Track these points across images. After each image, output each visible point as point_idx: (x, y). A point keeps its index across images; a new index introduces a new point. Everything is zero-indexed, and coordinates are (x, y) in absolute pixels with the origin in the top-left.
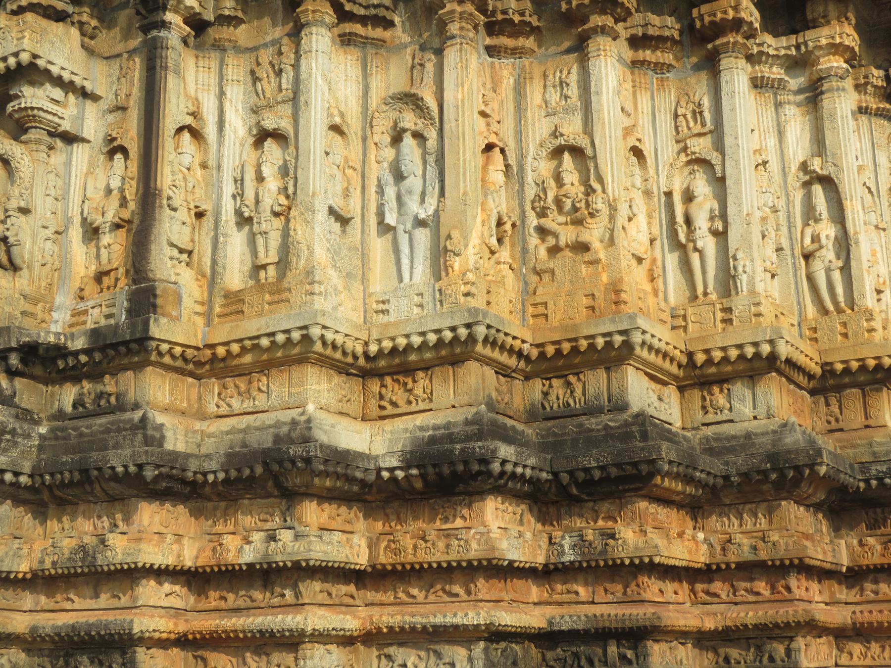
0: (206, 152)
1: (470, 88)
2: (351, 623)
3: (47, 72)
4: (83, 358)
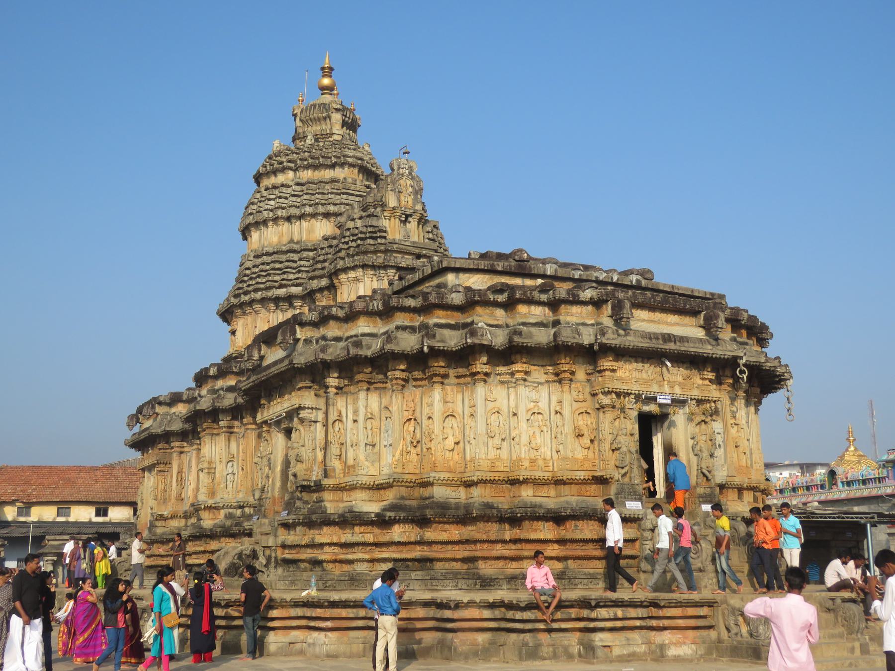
0: (344, 424)
2: (367, 556)
3: (305, 407)
4: (314, 488)
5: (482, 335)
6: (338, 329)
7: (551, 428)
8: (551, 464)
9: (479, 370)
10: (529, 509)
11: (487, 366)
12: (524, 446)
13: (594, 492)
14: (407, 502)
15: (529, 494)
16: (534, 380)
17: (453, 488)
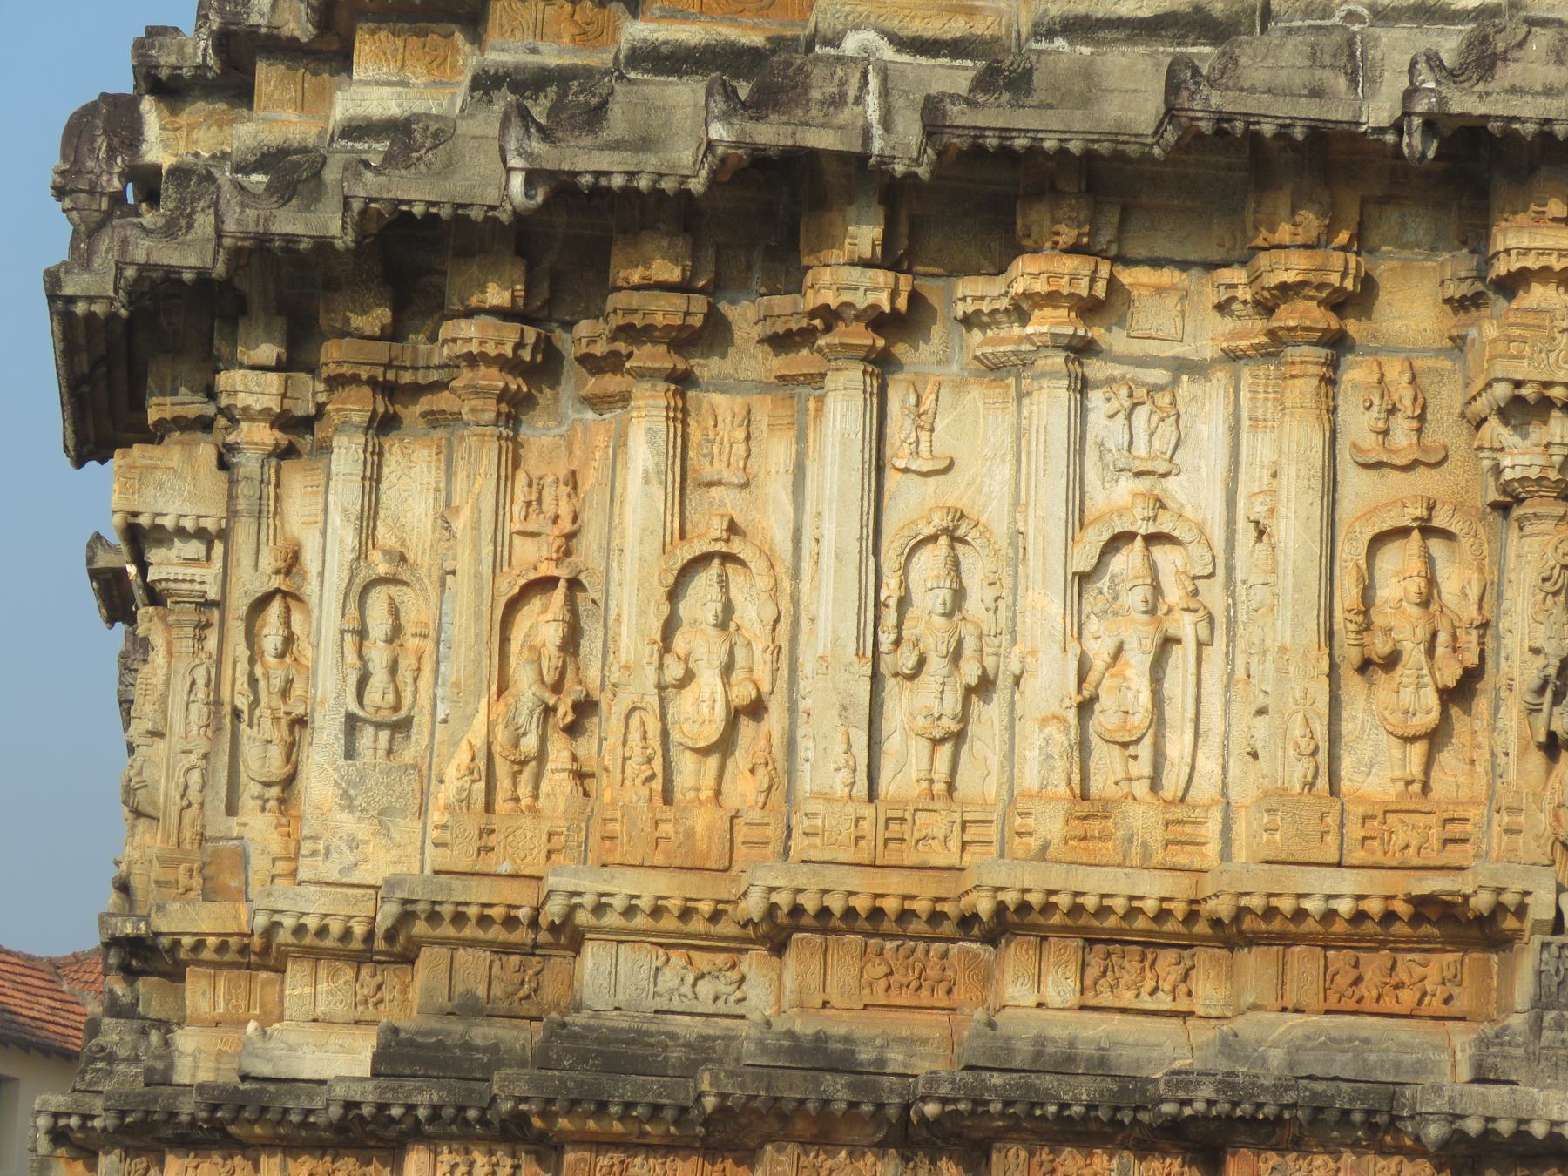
1: (477, 509)
5: (838, 101)
6: (301, 105)
7: (1231, 623)
8: (1212, 829)
9: (830, 298)
10: (997, 1080)
11: (882, 277)
12: (1044, 722)
13: (1441, 992)
14: (483, 1033)
15: (1051, 994)
16: (1152, 348)
17: (703, 960)
